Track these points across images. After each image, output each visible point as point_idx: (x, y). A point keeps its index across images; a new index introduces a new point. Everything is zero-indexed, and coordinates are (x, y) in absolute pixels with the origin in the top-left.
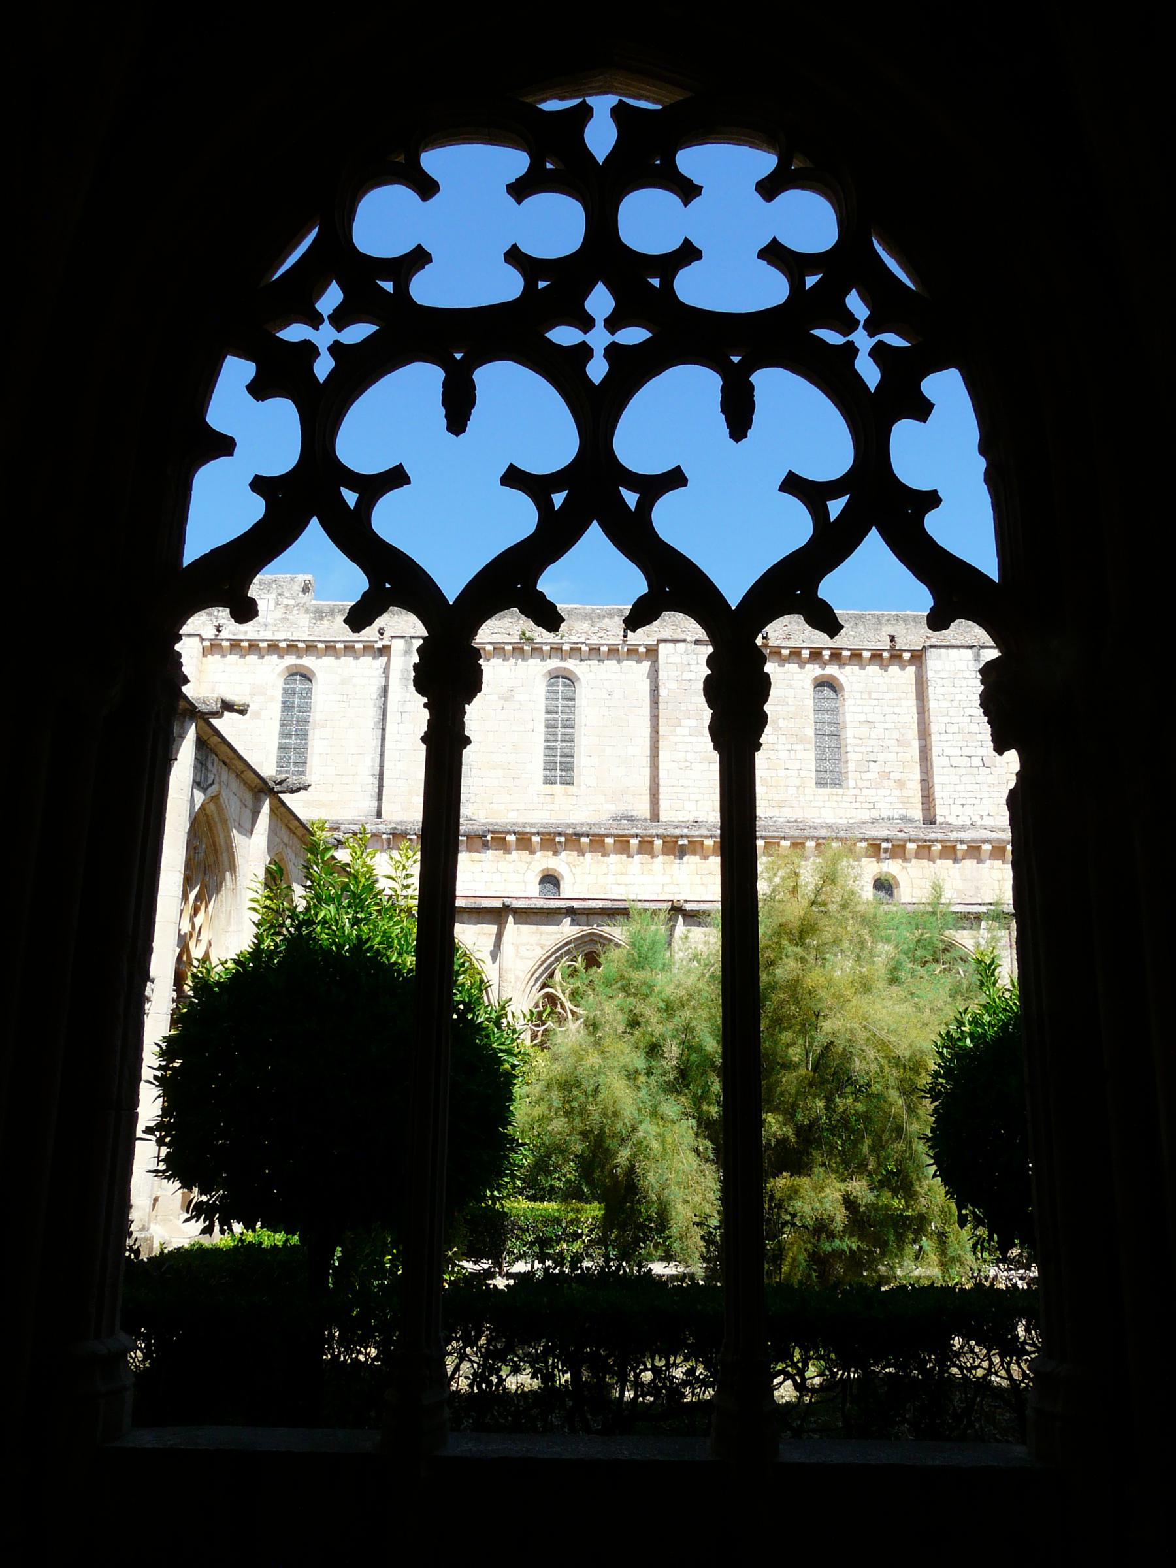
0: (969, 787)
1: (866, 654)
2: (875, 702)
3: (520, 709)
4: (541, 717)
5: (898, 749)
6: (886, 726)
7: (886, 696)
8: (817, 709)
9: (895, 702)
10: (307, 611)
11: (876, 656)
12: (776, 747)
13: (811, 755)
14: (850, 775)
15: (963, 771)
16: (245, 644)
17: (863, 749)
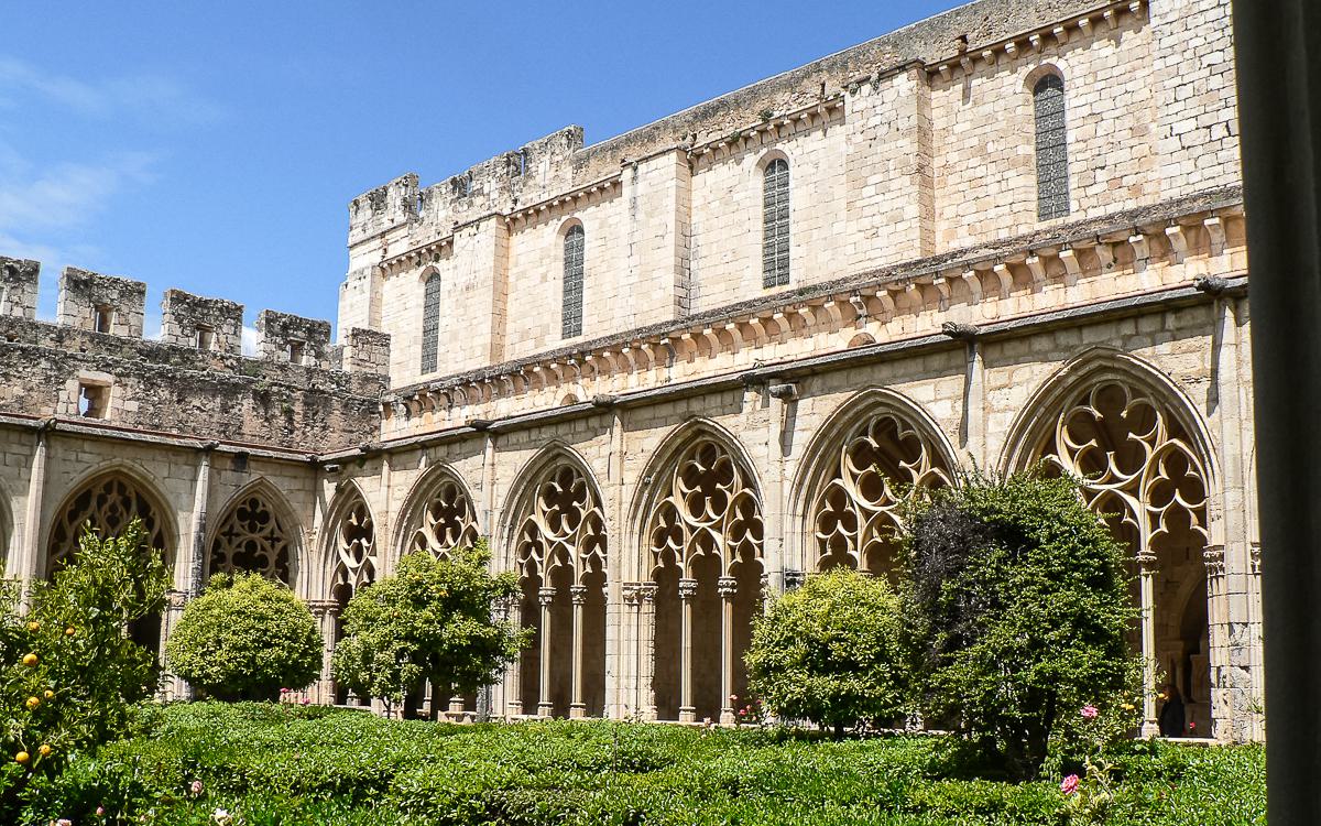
0: (1208, 173)
1: (1083, 22)
2: (1103, 84)
3: (737, 210)
4: (760, 211)
5: (1132, 142)
6: (1117, 113)
7: (1116, 72)
8: (1039, 114)
9: (1128, 75)
10: (571, 164)
11: (1097, 20)
12: (984, 181)
13: (1032, 180)
14: (1073, 195)
15: (1200, 150)
16: (556, 203)
17: (1088, 155)
